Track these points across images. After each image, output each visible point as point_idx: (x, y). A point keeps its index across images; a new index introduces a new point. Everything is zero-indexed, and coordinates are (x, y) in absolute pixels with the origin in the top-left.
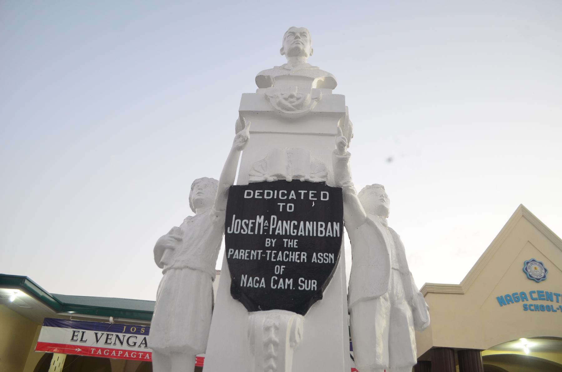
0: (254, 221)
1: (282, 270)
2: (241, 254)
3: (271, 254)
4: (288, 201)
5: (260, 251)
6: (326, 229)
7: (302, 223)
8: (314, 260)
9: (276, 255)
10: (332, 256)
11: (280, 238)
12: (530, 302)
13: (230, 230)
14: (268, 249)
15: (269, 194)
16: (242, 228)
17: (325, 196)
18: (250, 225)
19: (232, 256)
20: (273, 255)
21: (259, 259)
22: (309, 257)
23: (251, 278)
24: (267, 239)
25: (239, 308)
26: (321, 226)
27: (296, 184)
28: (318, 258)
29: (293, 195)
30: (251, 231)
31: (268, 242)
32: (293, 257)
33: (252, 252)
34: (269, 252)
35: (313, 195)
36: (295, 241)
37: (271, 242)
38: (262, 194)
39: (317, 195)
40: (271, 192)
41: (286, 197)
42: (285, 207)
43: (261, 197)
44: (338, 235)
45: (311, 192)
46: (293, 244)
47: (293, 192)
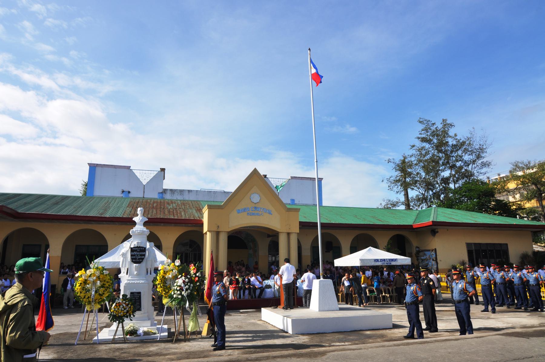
11: (137, 255)
12: (251, 212)
27: (140, 247)
28: (142, 257)
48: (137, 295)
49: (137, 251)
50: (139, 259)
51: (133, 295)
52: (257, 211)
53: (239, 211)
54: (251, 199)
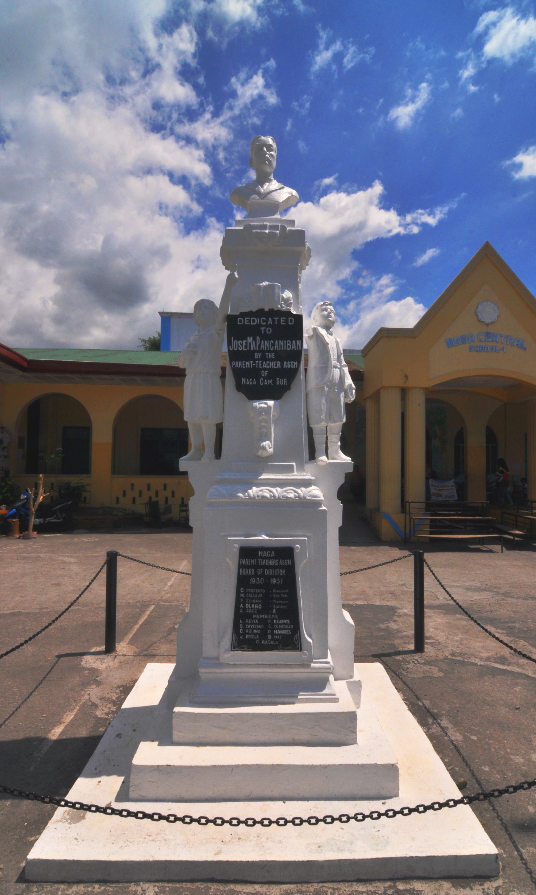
0: (246, 341)
1: (266, 373)
2: (240, 364)
3: (258, 363)
4: (266, 326)
5: (252, 362)
6: (292, 344)
7: (276, 342)
8: (285, 366)
9: (262, 363)
10: (296, 363)
11: (263, 352)
13: (231, 348)
14: (257, 360)
15: (254, 321)
16: (238, 346)
17: (291, 322)
18: (244, 344)
19: (234, 366)
20: (260, 364)
21: (252, 367)
22: (282, 365)
23: (248, 380)
24: (256, 354)
25: (242, 397)
26: (289, 343)
28: (287, 365)
29: (270, 321)
30: (245, 348)
31: (256, 355)
32: (272, 365)
33: (247, 363)
34: (257, 362)
35: (283, 321)
36: (273, 354)
37: (258, 355)
38: (250, 321)
39: (286, 321)
40: (256, 319)
41: (265, 323)
42: (265, 330)
43: (249, 324)
44: (300, 349)
45: (282, 318)
46: (272, 356)
47: (270, 319)
48: (272, 563)
49: (259, 333)
50: (273, 374)
51: (253, 562)
52: (493, 341)
53: (450, 343)
54: (479, 314)
